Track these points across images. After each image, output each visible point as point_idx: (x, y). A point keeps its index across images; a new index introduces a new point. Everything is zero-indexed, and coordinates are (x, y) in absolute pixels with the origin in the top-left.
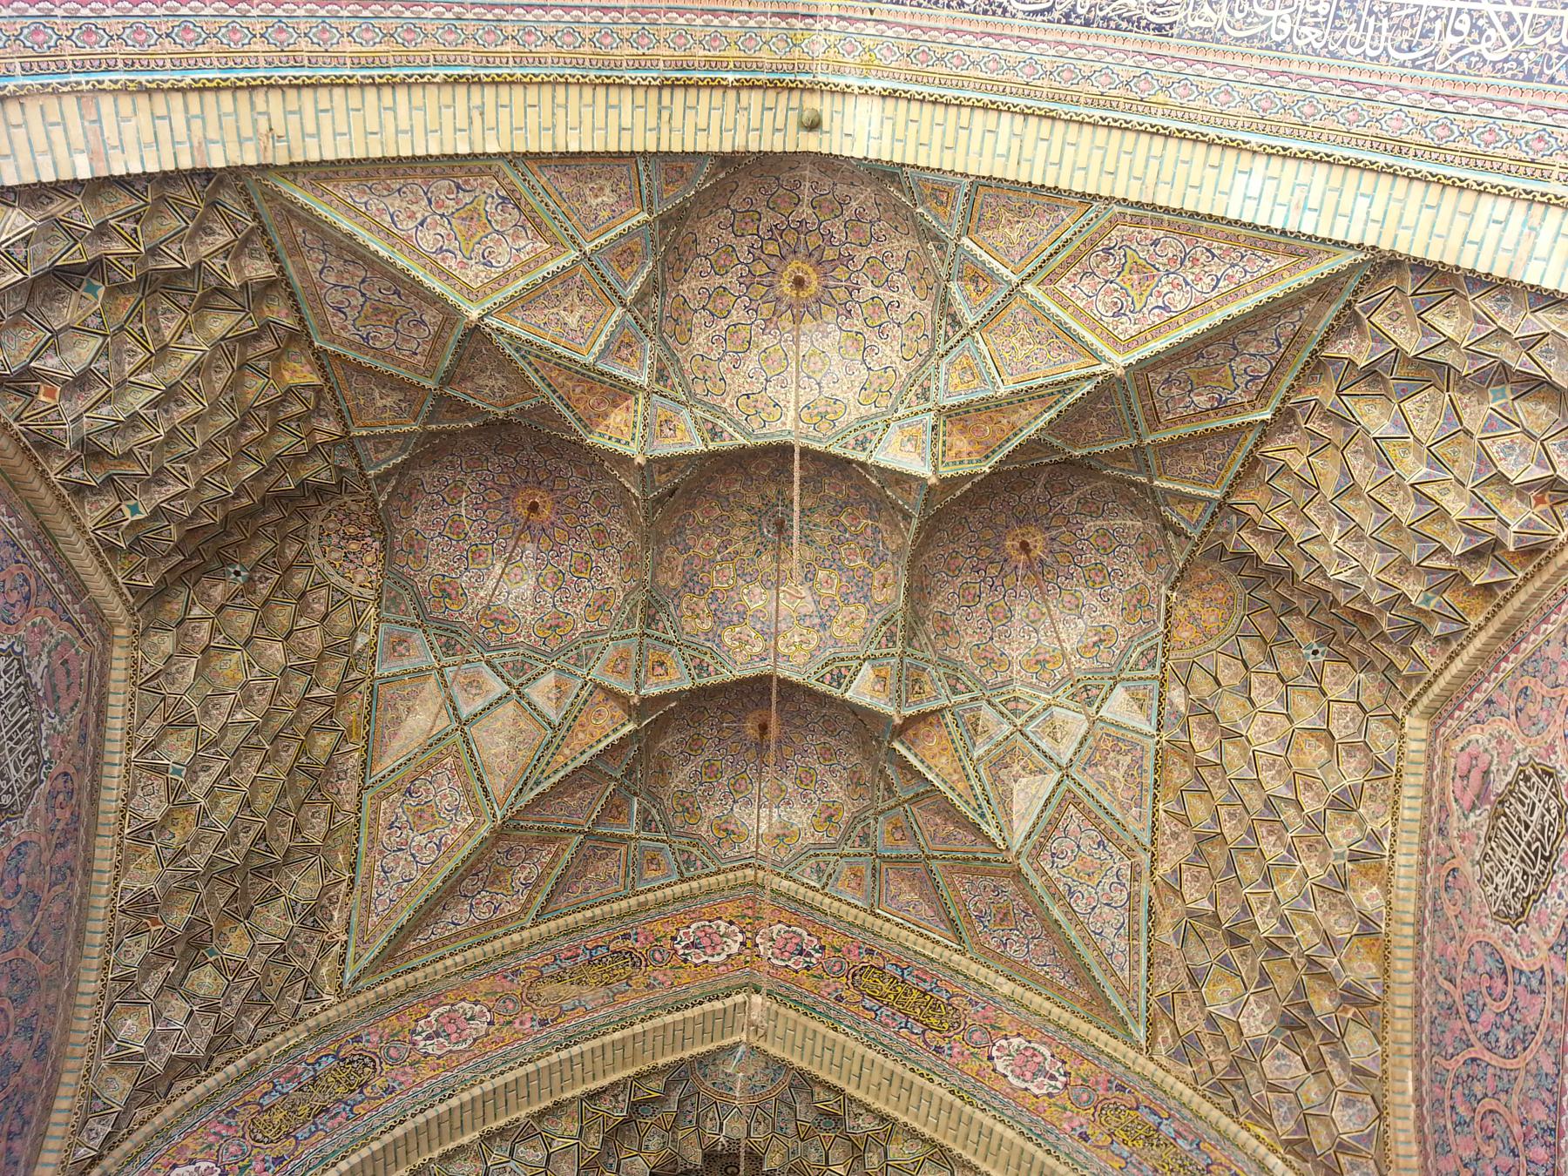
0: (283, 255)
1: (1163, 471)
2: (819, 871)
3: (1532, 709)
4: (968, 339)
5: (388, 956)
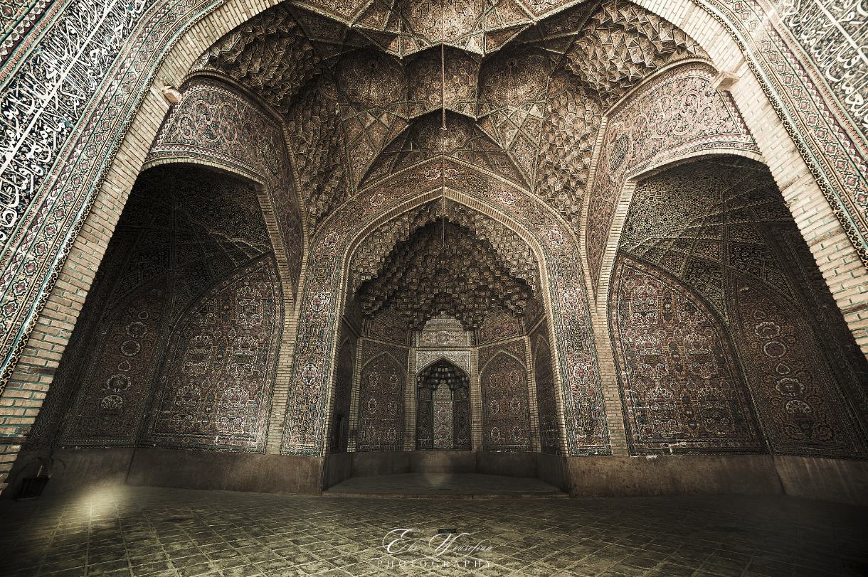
0: (297, 19)
1: (549, 47)
2: (459, 155)
3: (628, 121)
4: (492, 11)
5: (361, 186)
